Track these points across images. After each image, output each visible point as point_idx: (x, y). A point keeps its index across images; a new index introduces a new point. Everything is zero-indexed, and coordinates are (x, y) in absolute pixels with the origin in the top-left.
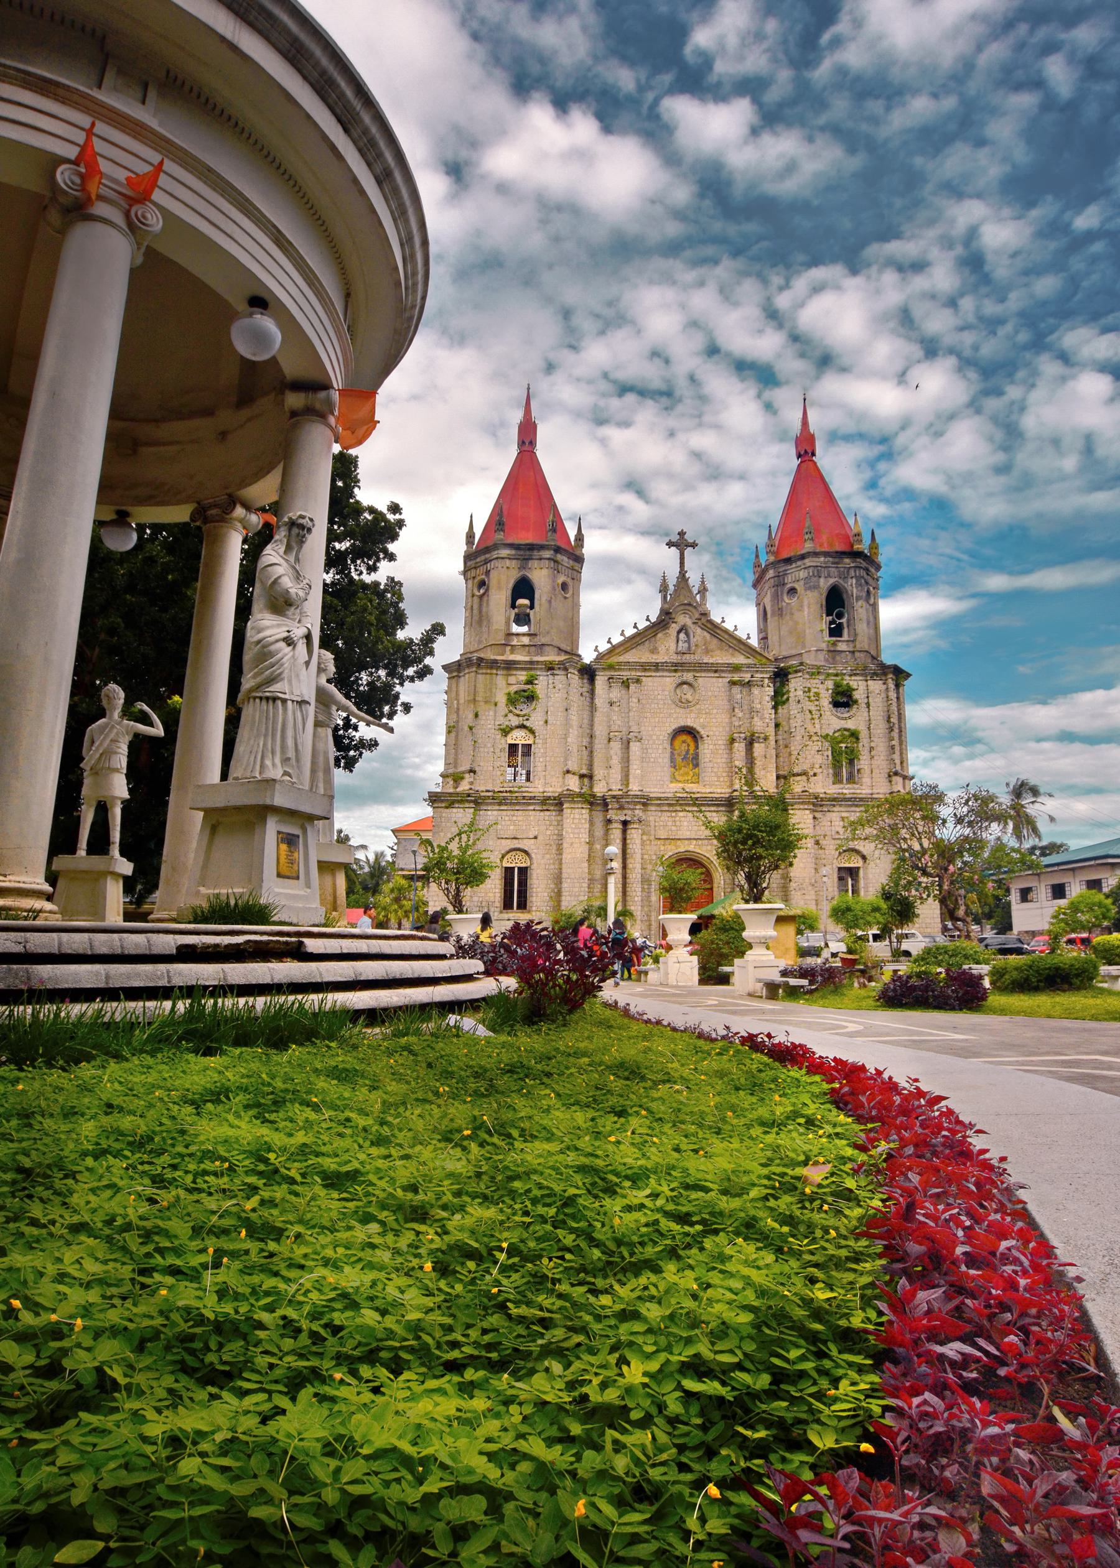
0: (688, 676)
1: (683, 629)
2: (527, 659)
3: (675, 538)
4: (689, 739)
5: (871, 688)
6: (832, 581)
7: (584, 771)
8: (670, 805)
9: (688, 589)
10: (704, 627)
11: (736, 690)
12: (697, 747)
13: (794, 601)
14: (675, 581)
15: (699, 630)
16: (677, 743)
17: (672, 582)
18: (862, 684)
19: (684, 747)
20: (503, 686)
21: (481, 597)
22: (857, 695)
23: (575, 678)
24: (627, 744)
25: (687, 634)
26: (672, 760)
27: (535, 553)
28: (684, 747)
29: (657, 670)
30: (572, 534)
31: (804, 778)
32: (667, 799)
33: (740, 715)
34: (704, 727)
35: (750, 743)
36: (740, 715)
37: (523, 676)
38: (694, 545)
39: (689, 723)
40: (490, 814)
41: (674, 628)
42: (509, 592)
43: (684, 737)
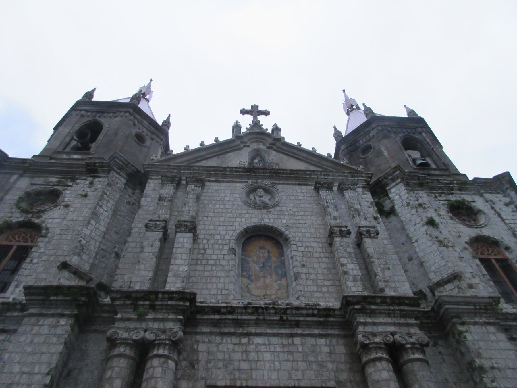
8: (238, 323)
10: (279, 151)
11: (323, 193)
15: (274, 153)
23: (121, 181)
32: (231, 310)
33: (335, 214)
34: (287, 227)
37: (54, 180)
38: (266, 113)
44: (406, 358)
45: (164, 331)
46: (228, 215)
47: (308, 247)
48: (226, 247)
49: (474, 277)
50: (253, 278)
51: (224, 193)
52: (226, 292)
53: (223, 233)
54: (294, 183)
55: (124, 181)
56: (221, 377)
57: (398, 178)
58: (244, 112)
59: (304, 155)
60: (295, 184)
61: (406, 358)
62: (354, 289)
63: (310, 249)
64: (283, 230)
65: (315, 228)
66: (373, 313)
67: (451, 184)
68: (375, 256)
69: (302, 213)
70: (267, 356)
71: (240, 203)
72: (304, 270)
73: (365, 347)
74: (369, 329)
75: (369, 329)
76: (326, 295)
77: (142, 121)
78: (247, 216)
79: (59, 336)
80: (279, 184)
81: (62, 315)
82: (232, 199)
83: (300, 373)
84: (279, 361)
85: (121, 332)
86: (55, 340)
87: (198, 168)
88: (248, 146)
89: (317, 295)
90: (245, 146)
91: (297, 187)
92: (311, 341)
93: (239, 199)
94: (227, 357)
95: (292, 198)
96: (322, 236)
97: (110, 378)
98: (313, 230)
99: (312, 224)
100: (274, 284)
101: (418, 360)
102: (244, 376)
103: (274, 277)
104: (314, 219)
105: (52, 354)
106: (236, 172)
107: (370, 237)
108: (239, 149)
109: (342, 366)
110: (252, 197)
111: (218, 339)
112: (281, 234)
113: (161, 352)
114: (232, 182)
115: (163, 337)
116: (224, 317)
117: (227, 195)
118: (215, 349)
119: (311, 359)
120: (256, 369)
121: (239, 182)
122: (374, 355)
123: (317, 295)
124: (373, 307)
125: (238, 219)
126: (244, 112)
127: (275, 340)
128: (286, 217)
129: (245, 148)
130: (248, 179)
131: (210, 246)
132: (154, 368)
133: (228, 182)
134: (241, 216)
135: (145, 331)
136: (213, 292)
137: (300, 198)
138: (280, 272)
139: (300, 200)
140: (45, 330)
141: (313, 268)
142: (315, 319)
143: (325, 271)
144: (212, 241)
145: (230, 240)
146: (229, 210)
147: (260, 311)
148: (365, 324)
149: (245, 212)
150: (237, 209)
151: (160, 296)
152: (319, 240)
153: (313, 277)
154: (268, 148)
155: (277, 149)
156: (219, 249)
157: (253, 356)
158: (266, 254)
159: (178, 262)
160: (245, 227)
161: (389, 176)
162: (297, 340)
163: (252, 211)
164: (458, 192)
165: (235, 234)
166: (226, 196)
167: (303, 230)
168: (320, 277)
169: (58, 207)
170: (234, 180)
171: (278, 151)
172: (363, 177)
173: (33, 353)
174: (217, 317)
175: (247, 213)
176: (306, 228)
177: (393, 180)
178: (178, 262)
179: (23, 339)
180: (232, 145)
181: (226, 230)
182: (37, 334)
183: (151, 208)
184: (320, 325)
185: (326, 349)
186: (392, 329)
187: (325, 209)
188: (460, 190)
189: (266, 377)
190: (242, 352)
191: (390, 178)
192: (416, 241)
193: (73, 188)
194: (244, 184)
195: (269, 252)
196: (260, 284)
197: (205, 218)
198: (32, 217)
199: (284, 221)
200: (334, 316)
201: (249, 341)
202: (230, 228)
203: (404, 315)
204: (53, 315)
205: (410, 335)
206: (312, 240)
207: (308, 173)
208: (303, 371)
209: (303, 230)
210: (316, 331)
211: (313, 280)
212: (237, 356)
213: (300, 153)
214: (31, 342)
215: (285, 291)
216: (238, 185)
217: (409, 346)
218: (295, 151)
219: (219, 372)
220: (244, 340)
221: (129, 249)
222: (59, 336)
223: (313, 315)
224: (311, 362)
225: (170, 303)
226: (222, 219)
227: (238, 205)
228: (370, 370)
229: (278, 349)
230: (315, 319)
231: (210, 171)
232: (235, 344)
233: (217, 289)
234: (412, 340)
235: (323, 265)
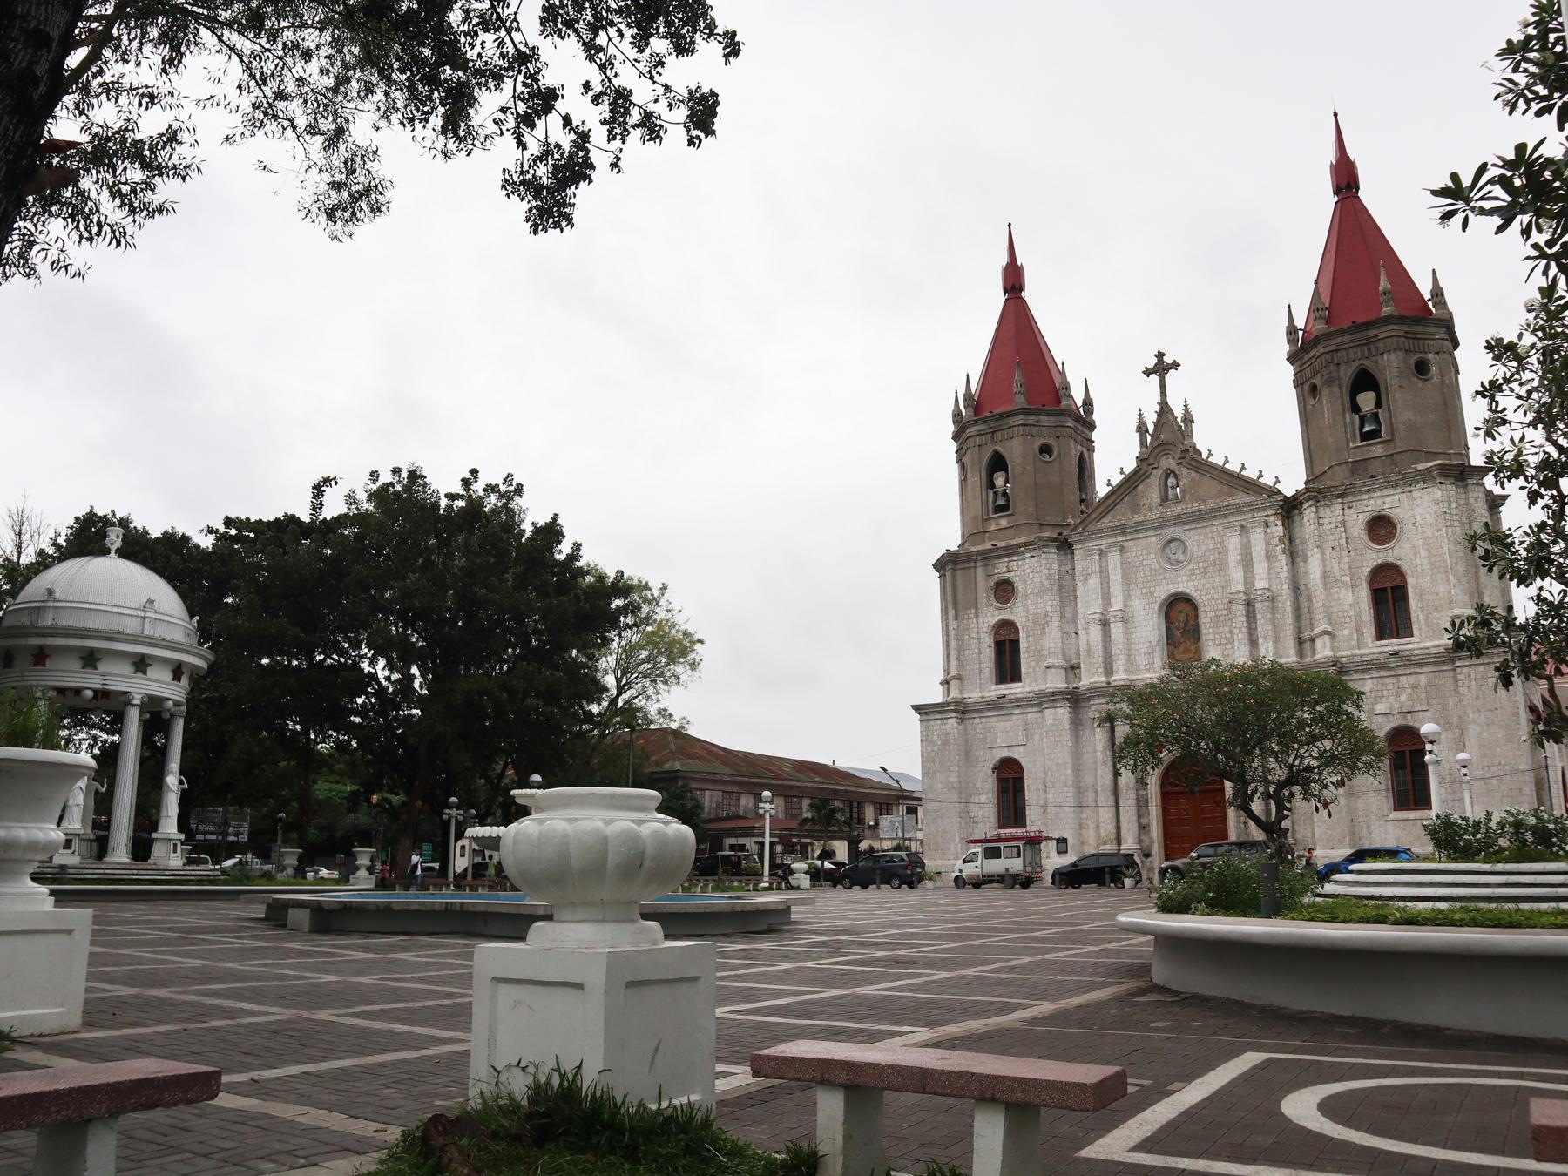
0: (1175, 531)
1: (1169, 473)
6: (1354, 365)
7: (1074, 662)
12: (1197, 616)
14: (1155, 417)
15: (1185, 471)
16: (1173, 613)
17: (1151, 419)
19: (1182, 618)
20: (983, 583)
25: (1176, 476)
27: (1004, 421)
31: (1327, 638)
38: (1175, 365)
40: (978, 723)
41: (1158, 473)
42: (984, 473)
43: (1182, 606)
47: (1215, 611)
55: (1055, 557)
58: (1148, 372)
59: (1216, 473)
63: (1218, 613)
71: (1157, 567)
77: (1039, 421)
82: (1150, 562)
103: (1192, 641)
110: (1167, 551)
126: (1148, 372)
128: (1198, 577)
129: (1155, 471)
154: (1178, 464)
160: (1163, 597)
165: (1156, 608)
171: (1189, 469)
175: (1165, 578)
180: (1139, 475)
193: (1019, 573)
195: (1187, 615)
196: (1181, 650)
199: (1196, 583)
213: (1212, 471)
216: (1153, 539)
218: (1207, 468)
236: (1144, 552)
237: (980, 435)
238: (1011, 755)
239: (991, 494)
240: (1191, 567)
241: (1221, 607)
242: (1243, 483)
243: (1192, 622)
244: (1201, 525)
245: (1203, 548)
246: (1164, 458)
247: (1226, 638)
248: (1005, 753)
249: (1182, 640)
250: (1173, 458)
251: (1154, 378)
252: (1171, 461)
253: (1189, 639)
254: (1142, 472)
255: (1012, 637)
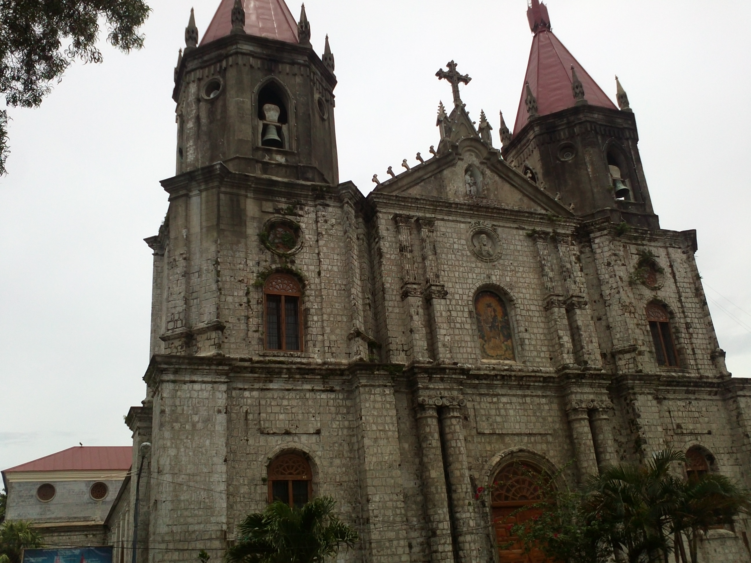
0: (488, 224)
2: (286, 180)
3: (446, 69)
4: (494, 303)
5: (673, 256)
9: (470, 124)
12: (505, 314)
13: (569, 159)
18: (662, 252)
19: (490, 312)
21: (212, 102)
22: (663, 262)
24: (428, 302)
26: (480, 329)
28: (490, 312)
29: (449, 213)
30: (320, 52)
33: (551, 274)
35: (570, 310)
36: (551, 274)
38: (466, 80)
39: (494, 279)
41: (461, 166)
42: (255, 97)
43: (487, 300)
44: (597, 417)
45: (453, 399)
46: (461, 269)
47: (528, 310)
48: (466, 309)
49: (644, 344)
50: (486, 338)
51: (452, 237)
52: (475, 357)
53: (460, 292)
54: (512, 225)
56: (486, 427)
57: (605, 229)
58: (440, 74)
60: (513, 228)
61: (597, 417)
62: (568, 361)
63: (530, 313)
64: (509, 291)
65: (533, 289)
66: (581, 385)
67: (644, 234)
68: (583, 329)
69: (521, 269)
70: (511, 412)
71: (469, 254)
72: (526, 336)
73: (575, 410)
74: (579, 397)
75: (579, 397)
76: (544, 360)
78: (477, 271)
79: (390, 403)
80: (499, 226)
81: (386, 386)
83: (532, 424)
84: (519, 416)
85: (426, 399)
86: (388, 406)
87: (425, 202)
88: (462, 160)
89: (538, 360)
90: (459, 159)
91: (515, 232)
92: (537, 400)
93: (466, 247)
94: (487, 413)
95: (512, 247)
96: (539, 298)
97: (430, 432)
98: (531, 291)
99: (530, 283)
100: (503, 345)
101: (605, 419)
102: (500, 427)
104: (532, 277)
105: (392, 416)
106: (460, 209)
107: (580, 308)
108: (454, 165)
109: (556, 419)
111: (478, 398)
112: (506, 293)
113: (456, 414)
114: (457, 221)
115: (455, 403)
116: (481, 382)
117: (456, 240)
118: (478, 407)
119: (538, 414)
120: (506, 422)
121: (463, 222)
122: (580, 416)
123: (538, 360)
124: (583, 381)
125: (470, 275)
126: (440, 74)
127: (514, 400)
128: (509, 274)
129: (460, 162)
130: (471, 217)
131: (453, 307)
132: (455, 425)
133: (453, 221)
134: (471, 270)
135: (441, 398)
136: (465, 356)
137: (519, 248)
138: (506, 333)
139: (519, 251)
140: (379, 399)
141: (534, 334)
142: (541, 384)
143: (542, 337)
144: (454, 302)
145: (468, 301)
146: (461, 262)
147: (506, 378)
148: (576, 393)
149: (474, 266)
150: (467, 261)
151: (447, 371)
152: (536, 303)
153: (533, 342)
154: (482, 163)
155: (492, 168)
156: (461, 311)
157: (503, 412)
158: (493, 313)
159: (443, 332)
161: (597, 224)
162: (528, 400)
163: (479, 265)
164: (648, 243)
165: (471, 294)
166: (454, 243)
167: (524, 291)
168: (539, 343)
169: (304, 250)
170: (458, 219)
172: (574, 223)
173: (378, 416)
174: (477, 382)
176: (526, 288)
177: (600, 230)
178: (443, 332)
179: (367, 405)
181: (463, 289)
182: (375, 401)
183: (393, 257)
184: (542, 387)
185: (547, 407)
186: (592, 397)
187: (542, 266)
188: (650, 240)
189: (513, 427)
190: (496, 409)
191: (597, 226)
192: (609, 306)
193: (305, 220)
194: (468, 225)
195: (495, 311)
196: (491, 344)
197: (443, 273)
198: (287, 262)
199: (508, 279)
200: (553, 383)
201: (498, 400)
202: (465, 286)
203: (600, 386)
204: (379, 386)
205: (602, 401)
206: (530, 302)
207: (527, 215)
208: (534, 423)
209: (524, 291)
210: (540, 393)
211: (535, 346)
212: (493, 412)
214: (374, 408)
215: (510, 352)
216: (462, 226)
217: (601, 409)
218: (511, 175)
219: (484, 424)
220: (495, 400)
221: (390, 309)
222: (390, 403)
223: (540, 381)
224: (538, 417)
225: (454, 376)
226: (457, 275)
227: (467, 256)
228: (576, 425)
229: (518, 407)
230: (541, 384)
231: (436, 206)
232: (490, 403)
233: (467, 353)
234: (604, 406)
235: (541, 331)
236: (455, 235)
237: (253, 57)
238: (292, 445)
239: (261, 124)
240: (501, 261)
241: (533, 308)
242: (545, 200)
243: (499, 318)
244: (508, 225)
245: (512, 247)
246: (468, 153)
247: (541, 340)
248: (290, 443)
249: (491, 335)
250: (477, 156)
251: (446, 85)
252: (474, 159)
253: (499, 335)
254: (451, 158)
255: (291, 292)
